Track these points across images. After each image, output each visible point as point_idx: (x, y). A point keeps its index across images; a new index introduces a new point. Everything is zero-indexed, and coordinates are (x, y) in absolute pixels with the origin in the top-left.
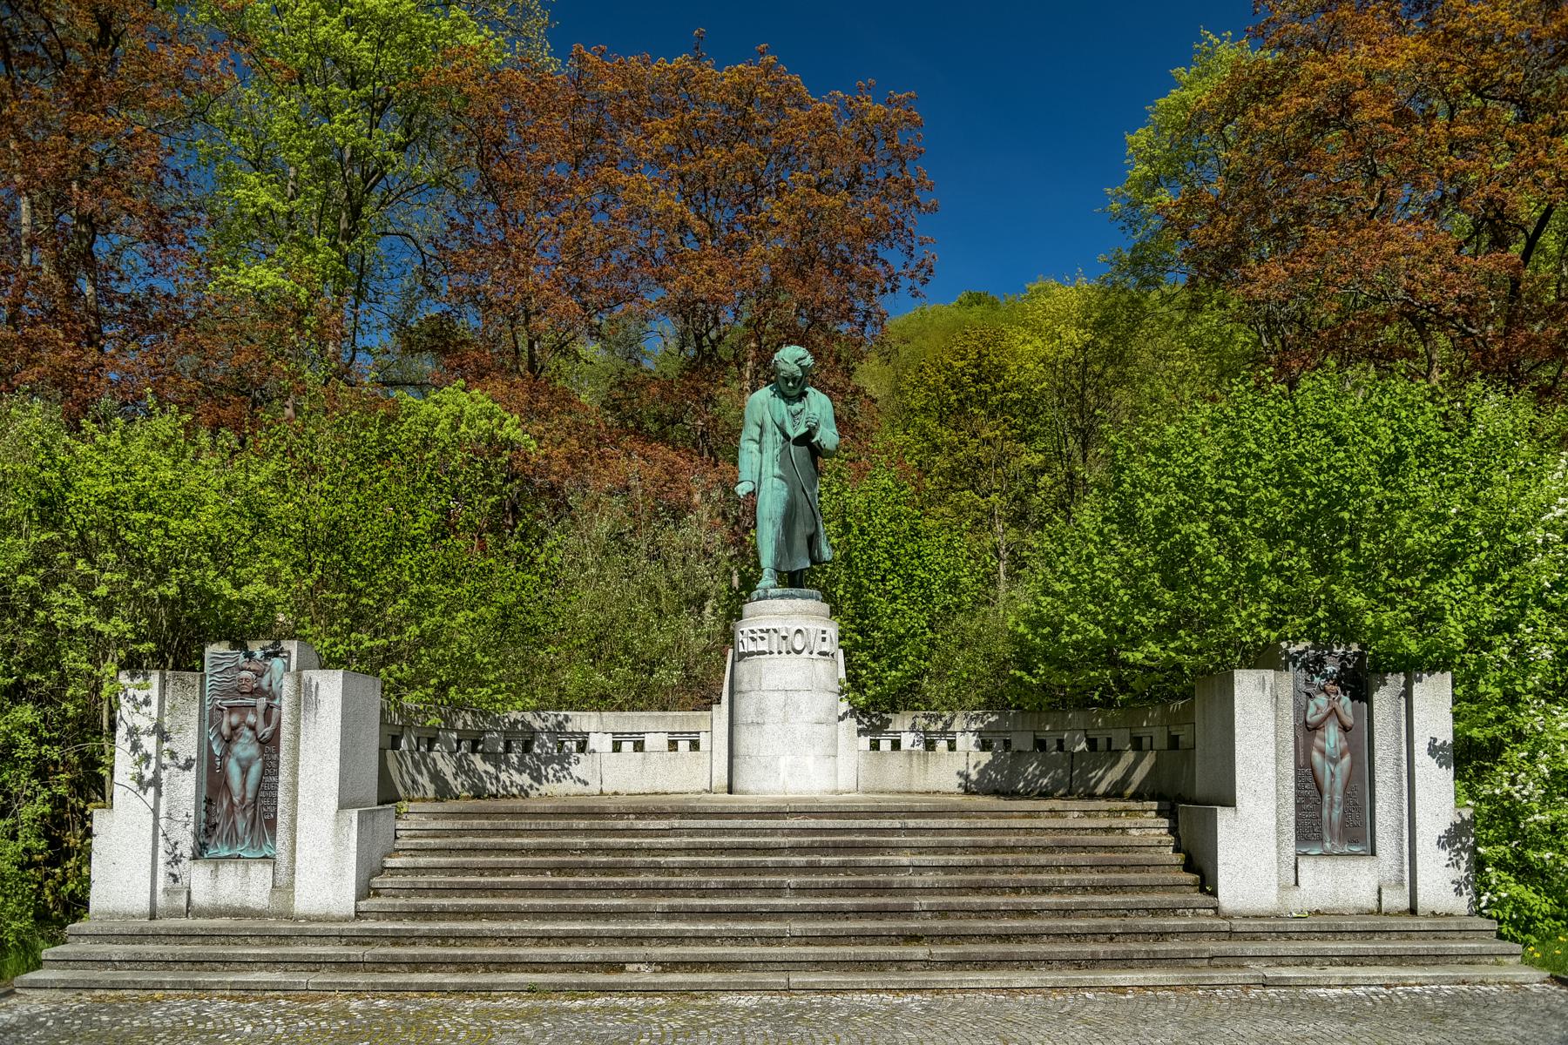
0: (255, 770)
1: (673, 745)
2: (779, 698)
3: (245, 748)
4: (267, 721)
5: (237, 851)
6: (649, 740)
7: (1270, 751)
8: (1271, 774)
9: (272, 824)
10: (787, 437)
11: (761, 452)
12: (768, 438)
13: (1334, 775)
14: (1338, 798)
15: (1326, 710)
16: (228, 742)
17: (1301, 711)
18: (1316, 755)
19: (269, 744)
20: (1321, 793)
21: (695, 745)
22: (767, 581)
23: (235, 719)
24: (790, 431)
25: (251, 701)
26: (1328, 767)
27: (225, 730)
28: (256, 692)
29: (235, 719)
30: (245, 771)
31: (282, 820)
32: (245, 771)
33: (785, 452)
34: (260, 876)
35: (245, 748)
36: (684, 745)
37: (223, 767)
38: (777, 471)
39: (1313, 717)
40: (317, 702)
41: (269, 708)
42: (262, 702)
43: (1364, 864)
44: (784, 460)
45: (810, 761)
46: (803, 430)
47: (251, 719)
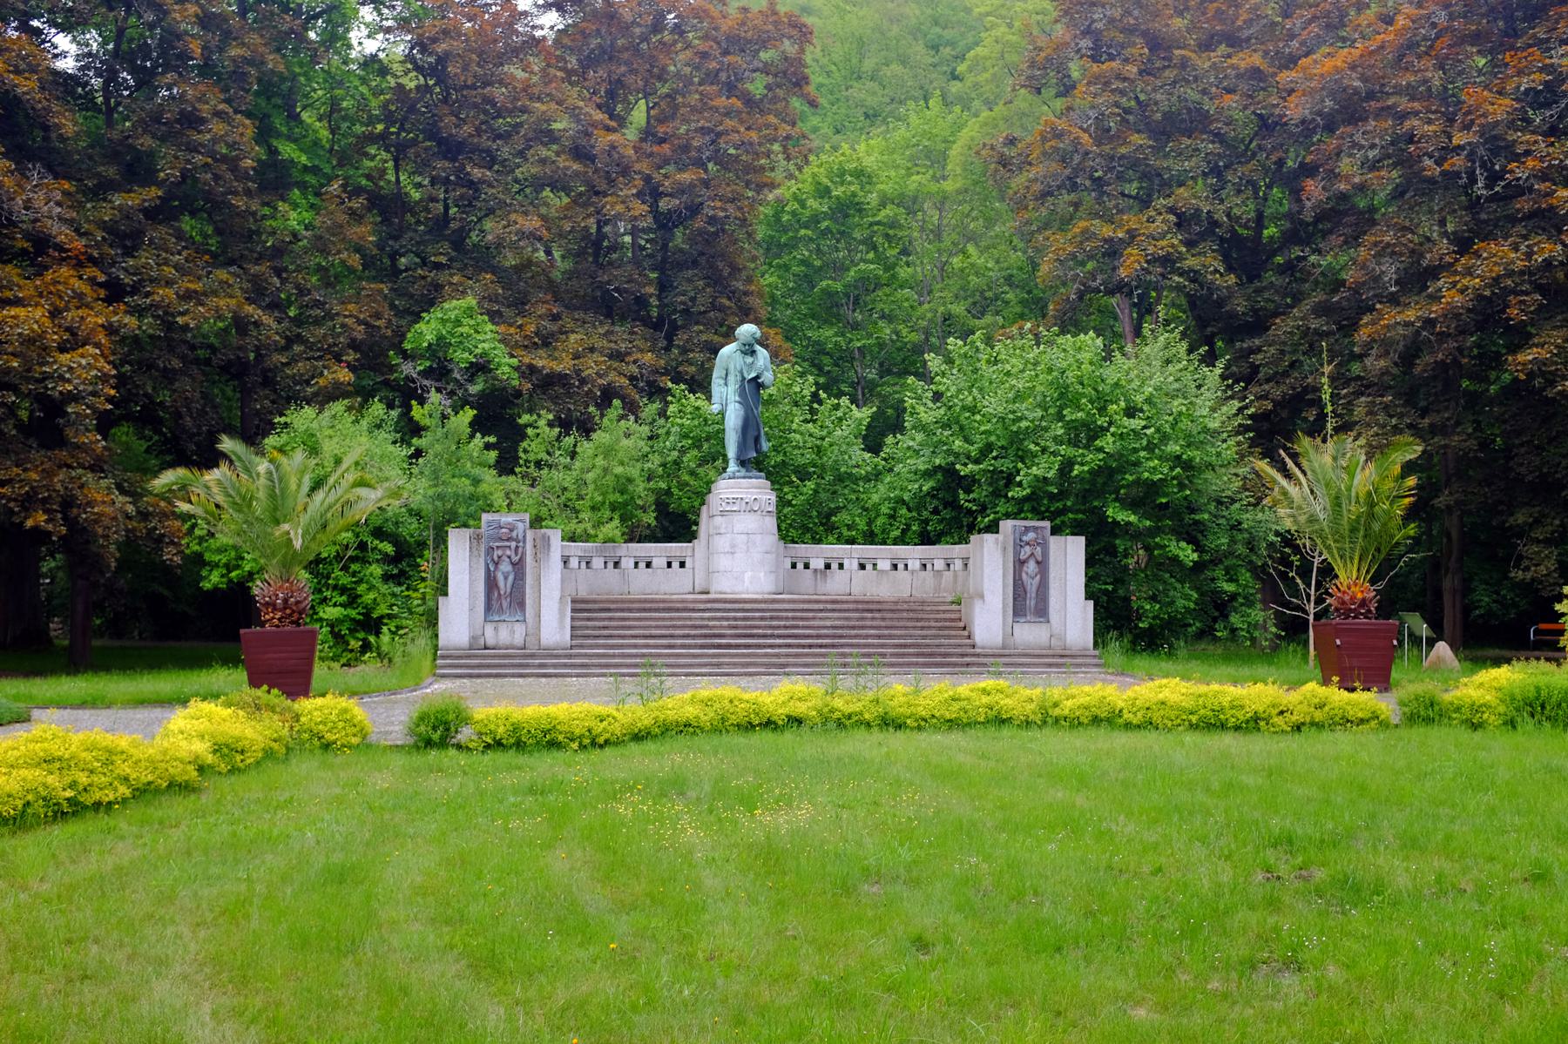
0: (511, 578)
1: (669, 565)
2: (744, 537)
3: (505, 567)
4: (516, 554)
5: (502, 618)
6: (655, 562)
7: (1001, 572)
8: (1000, 583)
9: (522, 605)
10: (744, 379)
11: (726, 384)
12: (731, 378)
13: (1032, 585)
14: (1034, 595)
15: (1029, 553)
16: (497, 564)
17: (1016, 554)
18: (1024, 576)
19: (519, 566)
20: (1026, 593)
21: (682, 565)
22: (733, 467)
23: (500, 552)
24: (746, 375)
25: (507, 544)
26: (1030, 581)
27: (496, 558)
28: (508, 540)
29: (500, 552)
30: (506, 578)
31: (529, 602)
32: (506, 578)
33: (742, 388)
34: (520, 630)
35: (505, 567)
36: (675, 565)
37: (495, 577)
38: (737, 398)
39: (1023, 557)
40: (549, 545)
41: (517, 547)
42: (513, 544)
43: (1044, 626)
44: (742, 392)
45: (762, 574)
46: (753, 375)
47: (508, 552)
